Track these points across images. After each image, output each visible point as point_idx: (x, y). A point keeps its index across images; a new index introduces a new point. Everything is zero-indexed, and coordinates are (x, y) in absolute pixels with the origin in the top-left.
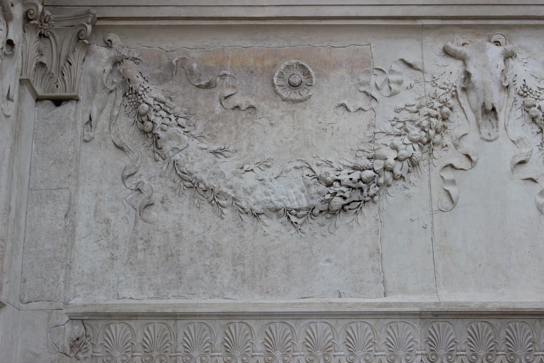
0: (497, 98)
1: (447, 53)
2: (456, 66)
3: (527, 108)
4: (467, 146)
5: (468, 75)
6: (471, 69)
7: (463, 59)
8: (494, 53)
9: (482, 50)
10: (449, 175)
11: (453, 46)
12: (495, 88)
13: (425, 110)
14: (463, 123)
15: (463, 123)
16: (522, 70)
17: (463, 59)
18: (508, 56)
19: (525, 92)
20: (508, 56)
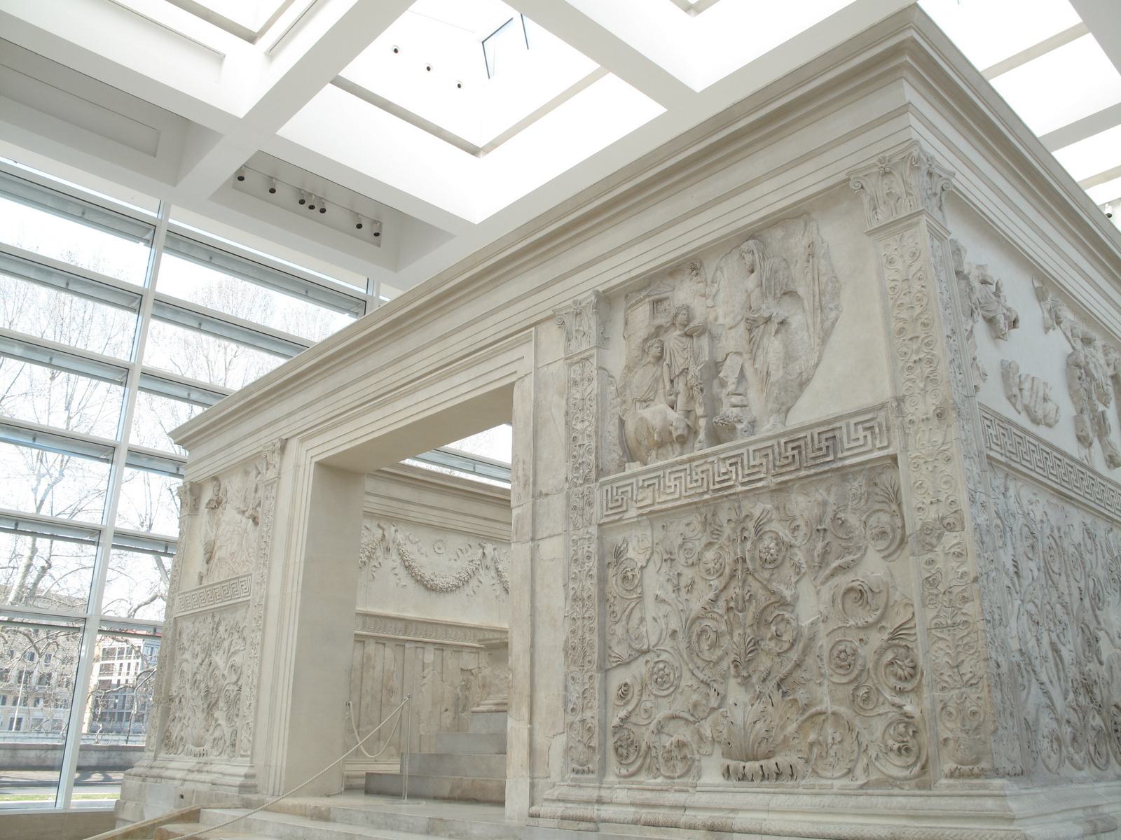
0: (391, 545)
1: (379, 526)
2: (381, 532)
3: (399, 550)
4: (380, 560)
5: (384, 536)
6: (386, 533)
7: (383, 530)
8: (393, 529)
9: (390, 528)
10: (374, 569)
11: (382, 525)
12: (391, 542)
13: (371, 546)
14: (379, 553)
15: (379, 553)
16: (400, 536)
17: (383, 530)
18: (396, 531)
19: (399, 544)
20: (396, 531)
